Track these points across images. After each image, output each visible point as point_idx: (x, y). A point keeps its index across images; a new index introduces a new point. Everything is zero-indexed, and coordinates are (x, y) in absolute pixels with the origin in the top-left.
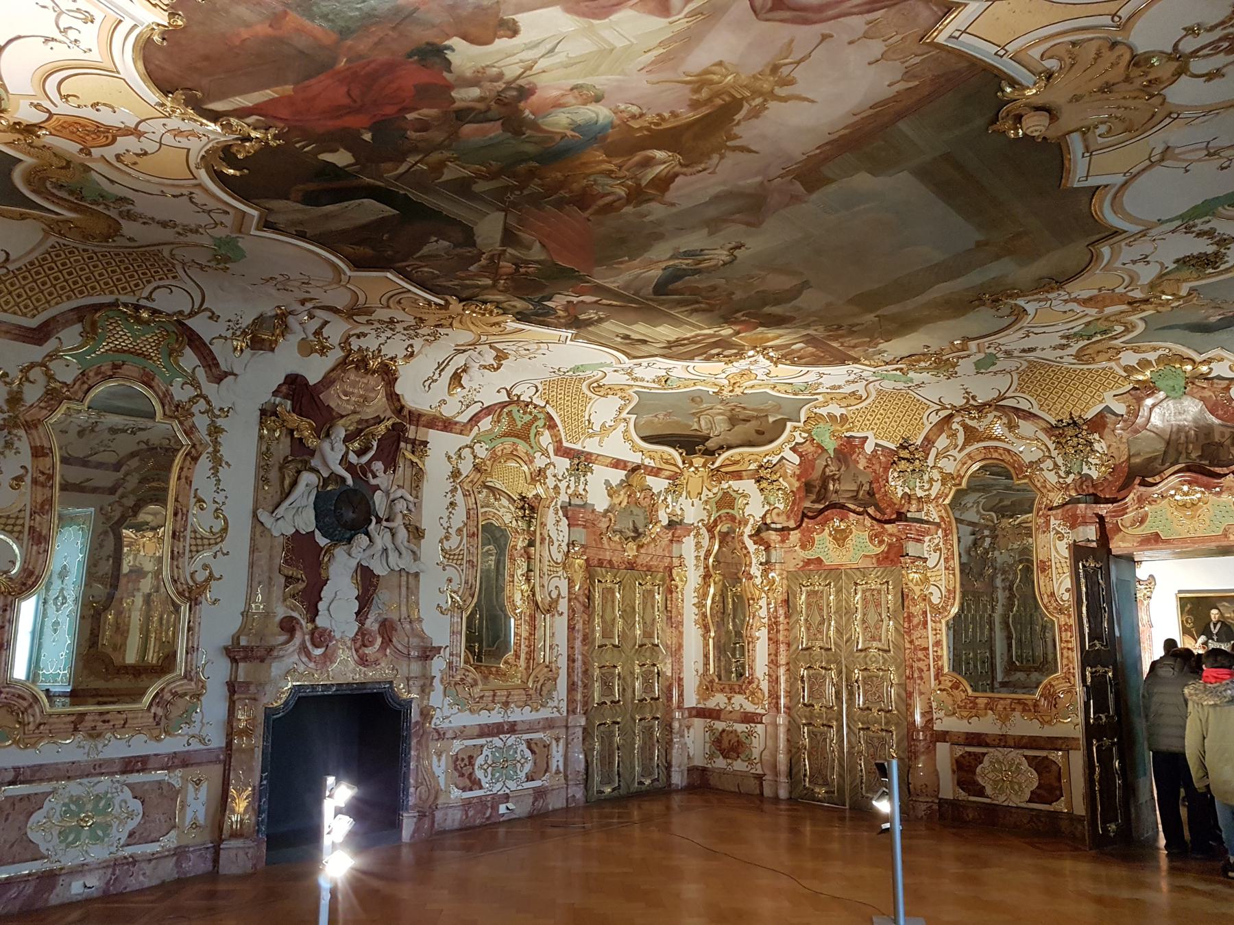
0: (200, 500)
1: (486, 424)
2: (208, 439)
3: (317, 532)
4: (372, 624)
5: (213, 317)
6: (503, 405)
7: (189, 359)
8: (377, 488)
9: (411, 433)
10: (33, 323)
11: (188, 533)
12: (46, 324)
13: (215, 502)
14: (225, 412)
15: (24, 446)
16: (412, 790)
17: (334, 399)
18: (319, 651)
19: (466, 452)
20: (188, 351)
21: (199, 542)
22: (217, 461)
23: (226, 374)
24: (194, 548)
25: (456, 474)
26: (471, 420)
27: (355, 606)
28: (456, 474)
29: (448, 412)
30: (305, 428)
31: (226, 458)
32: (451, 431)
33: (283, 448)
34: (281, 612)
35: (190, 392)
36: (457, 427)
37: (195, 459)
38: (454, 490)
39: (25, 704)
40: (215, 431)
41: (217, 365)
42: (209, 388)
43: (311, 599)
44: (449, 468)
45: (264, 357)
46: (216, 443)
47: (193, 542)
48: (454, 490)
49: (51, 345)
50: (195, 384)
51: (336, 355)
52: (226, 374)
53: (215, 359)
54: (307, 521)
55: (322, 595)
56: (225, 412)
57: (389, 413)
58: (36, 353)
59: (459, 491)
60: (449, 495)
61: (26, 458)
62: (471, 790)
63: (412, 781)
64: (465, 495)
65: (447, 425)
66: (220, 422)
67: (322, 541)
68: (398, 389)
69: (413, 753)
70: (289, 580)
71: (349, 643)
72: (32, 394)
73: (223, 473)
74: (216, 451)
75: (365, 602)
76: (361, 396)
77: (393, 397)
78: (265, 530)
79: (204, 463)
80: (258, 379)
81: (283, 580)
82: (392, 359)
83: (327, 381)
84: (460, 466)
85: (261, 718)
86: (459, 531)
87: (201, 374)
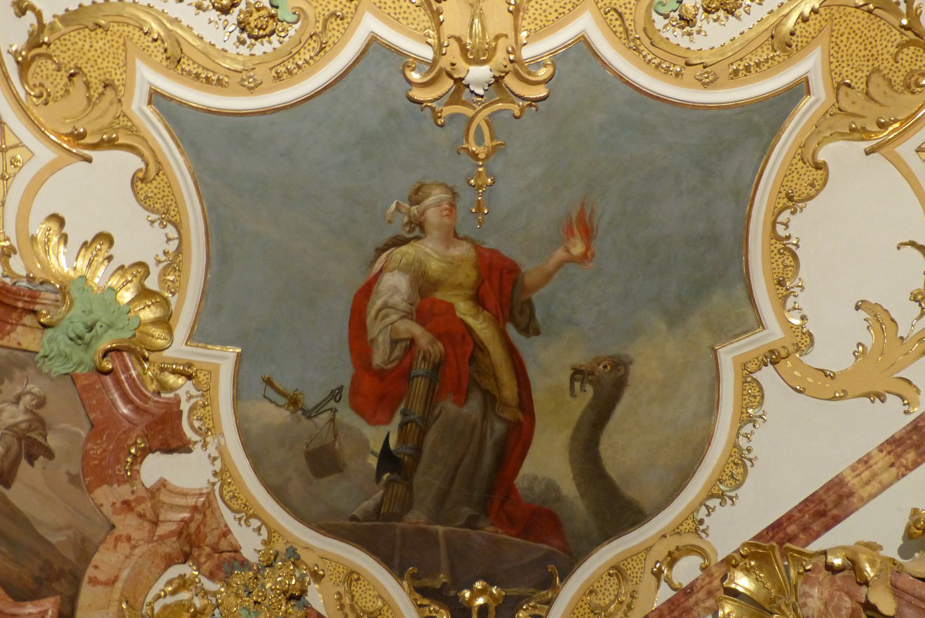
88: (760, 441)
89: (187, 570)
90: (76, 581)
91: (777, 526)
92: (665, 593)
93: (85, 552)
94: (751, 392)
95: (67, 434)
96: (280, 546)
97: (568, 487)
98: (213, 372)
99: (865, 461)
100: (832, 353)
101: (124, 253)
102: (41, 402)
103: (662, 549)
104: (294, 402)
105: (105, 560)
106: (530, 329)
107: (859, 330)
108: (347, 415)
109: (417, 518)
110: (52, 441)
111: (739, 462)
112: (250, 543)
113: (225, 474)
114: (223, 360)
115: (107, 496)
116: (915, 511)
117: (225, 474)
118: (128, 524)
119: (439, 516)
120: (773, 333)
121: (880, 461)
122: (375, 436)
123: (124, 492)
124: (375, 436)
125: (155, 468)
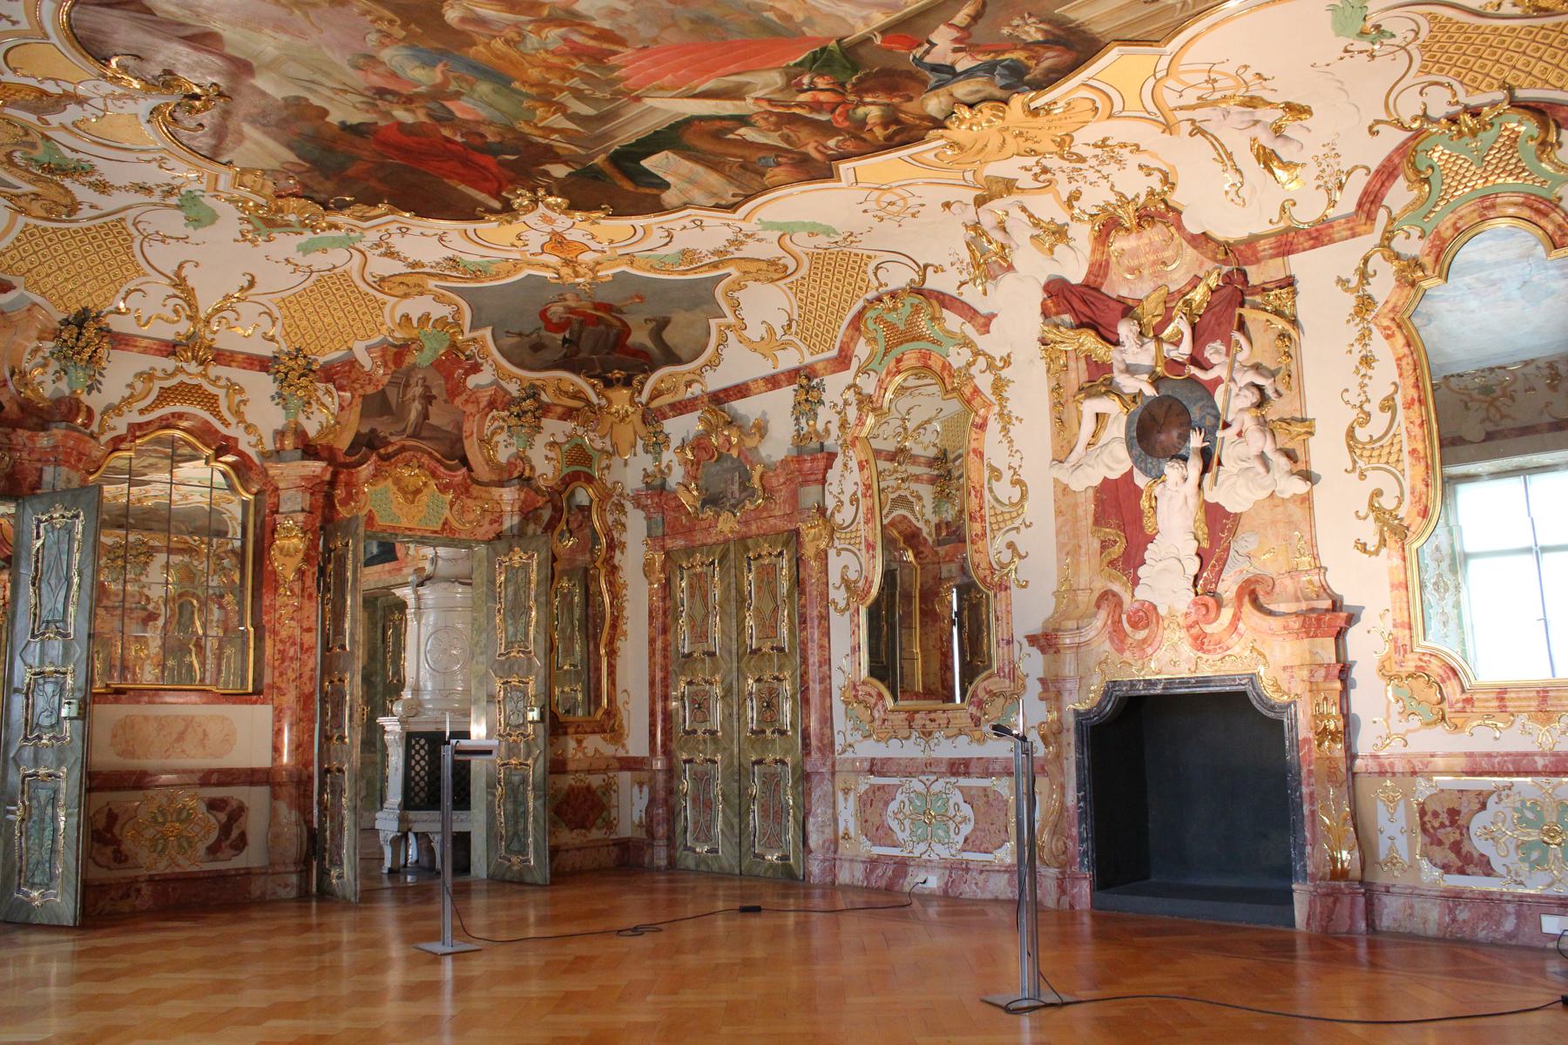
0: (993, 469)
1: (1399, 194)
2: (993, 398)
3: (1136, 470)
4: (1228, 586)
5: (938, 269)
6: (1403, 150)
7: (953, 321)
8: (1218, 381)
9: (1255, 275)
10: (834, 353)
11: (987, 511)
12: (841, 349)
13: (1010, 468)
14: (1007, 362)
15: (854, 464)
16: (1308, 849)
17: (1120, 286)
18: (1142, 634)
19: (1376, 262)
20: (946, 313)
21: (1000, 518)
22: (1006, 419)
23: (990, 317)
24: (995, 527)
25: (1365, 304)
26: (1360, 205)
27: (1193, 566)
28: (1365, 304)
29: (1307, 214)
30: (1089, 340)
31: (1014, 414)
32: (1332, 241)
33: (1078, 374)
34: (1100, 585)
35: (966, 354)
36: (1337, 228)
37: (982, 427)
38: (1364, 337)
39: (873, 701)
40: (999, 386)
41: (976, 312)
42: (982, 342)
43: (1130, 561)
44: (1351, 301)
45: (1007, 280)
46: (1002, 400)
47: (993, 520)
48: (1364, 337)
49: (855, 364)
50: (967, 343)
51: (1083, 235)
52: (990, 317)
53: (970, 308)
54: (1115, 460)
55: (1147, 555)
56: (1007, 362)
57: (1209, 265)
58: (846, 377)
59: (1377, 334)
60: (1358, 347)
61: (856, 476)
62: (1462, 872)
63: (1308, 835)
64: (1388, 337)
65: (1318, 235)
66: (1005, 373)
67: (1141, 480)
68: (1193, 228)
69: (1305, 790)
70: (1105, 545)
71: (1181, 620)
72: (852, 413)
73: (1015, 430)
74: (1002, 407)
75: (1211, 557)
76: (1154, 263)
77: (1202, 241)
78: (1066, 489)
79: (994, 426)
80: (1016, 309)
81: (1096, 545)
82: (1152, 193)
83: (1100, 269)
84: (1369, 290)
85: (1070, 721)
86: (1388, 405)
87: (970, 330)
88: (725, 352)
89: (495, 412)
90: (460, 440)
91: (725, 390)
92: (688, 395)
93: (459, 427)
94: (723, 342)
95: (438, 386)
96: (526, 384)
97: (650, 344)
98: (483, 337)
99: (755, 381)
100: (755, 332)
101: (434, 316)
102: (424, 379)
103: (689, 377)
104: (520, 335)
105: (467, 427)
106: (622, 312)
107: (762, 330)
108: (544, 333)
109: (583, 355)
110: (434, 392)
111: (718, 354)
112: (513, 389)
113: (498, 368)
114: (487, 333)
115: (458, 401)
116: (764, 413)
117: (498, 368)
118: (470, 408)
119: (593, 352)
120: (731, 319)
121: (761, 383)
122: (560, 336)
123: (464, 397)
124: (560, 336)
125: (472, 381)
